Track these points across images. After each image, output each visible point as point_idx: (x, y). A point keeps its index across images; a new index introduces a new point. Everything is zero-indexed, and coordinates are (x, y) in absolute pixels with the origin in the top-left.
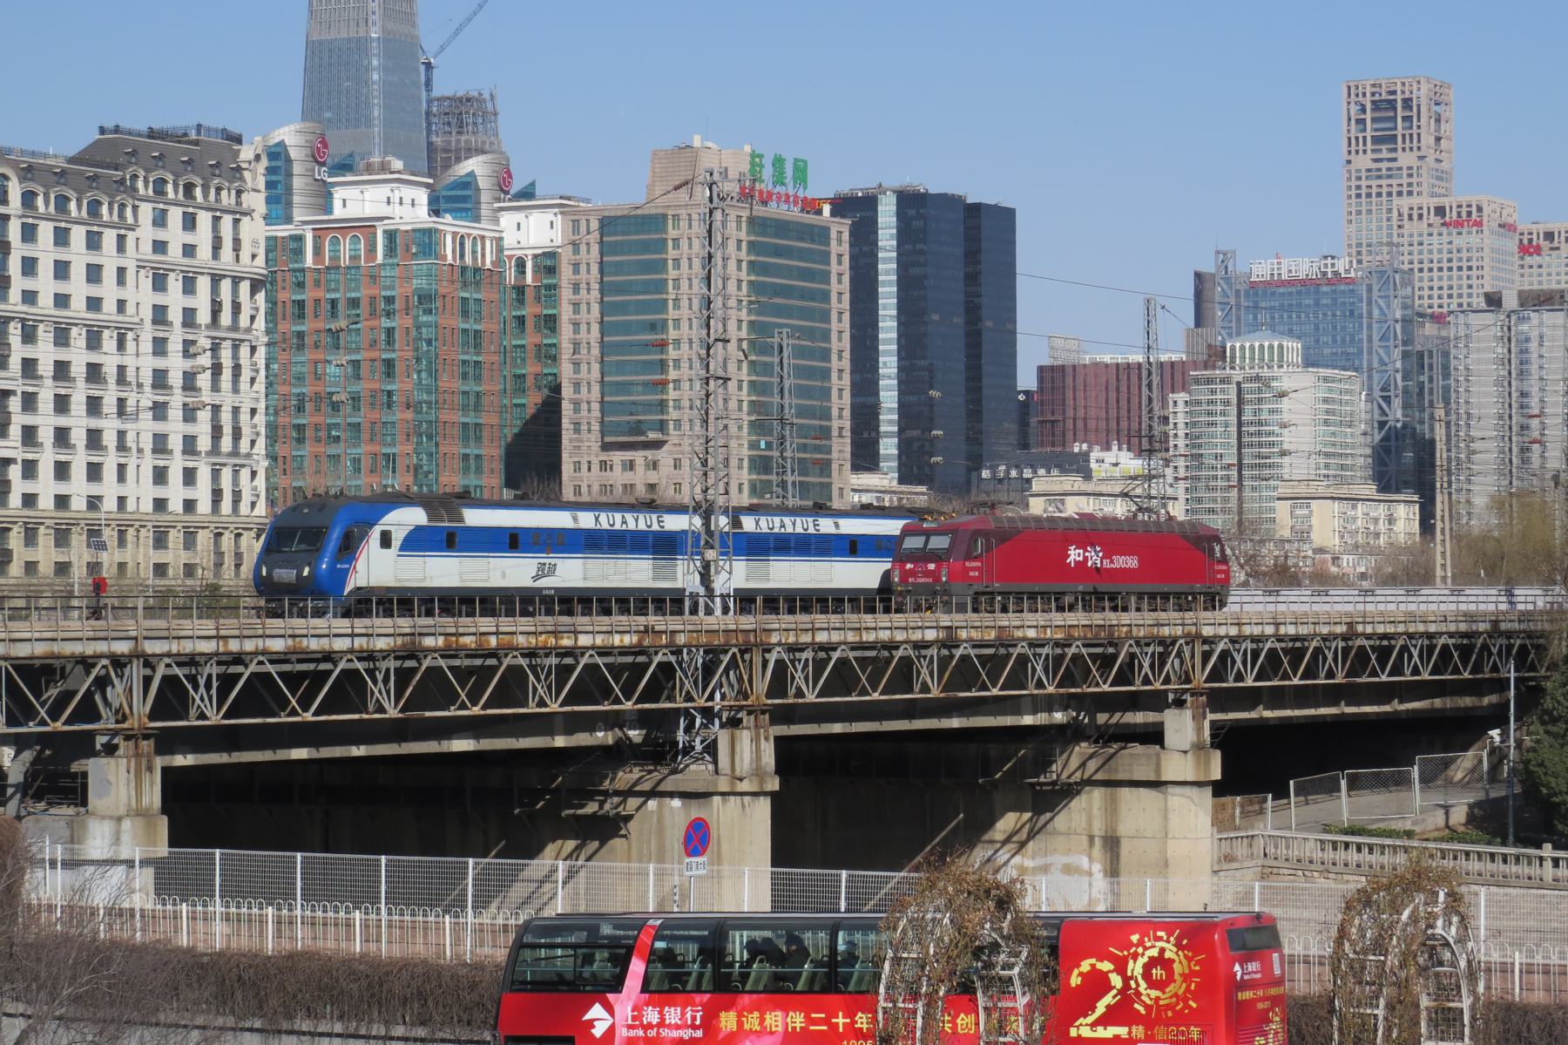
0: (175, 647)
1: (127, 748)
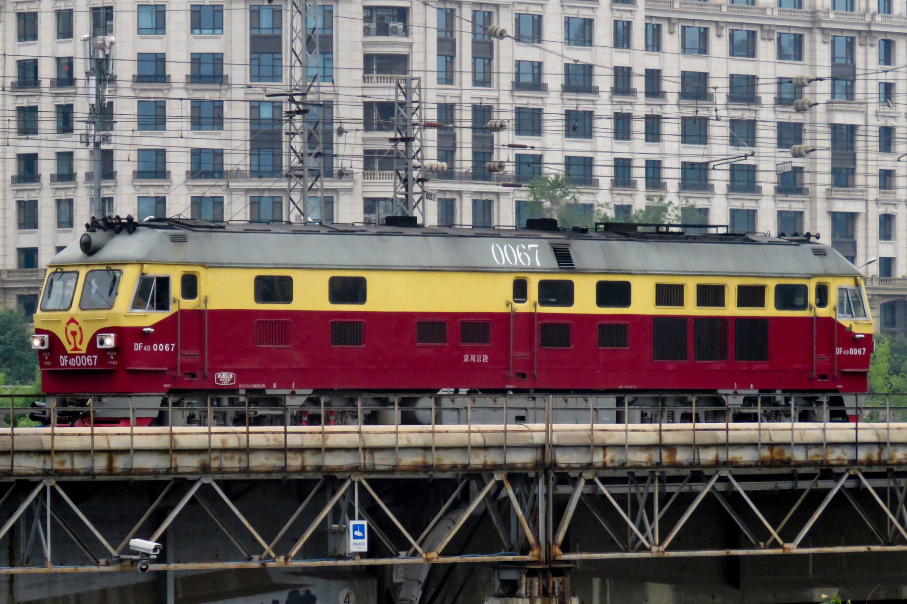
0: (598, 458)
1: (530, 587)
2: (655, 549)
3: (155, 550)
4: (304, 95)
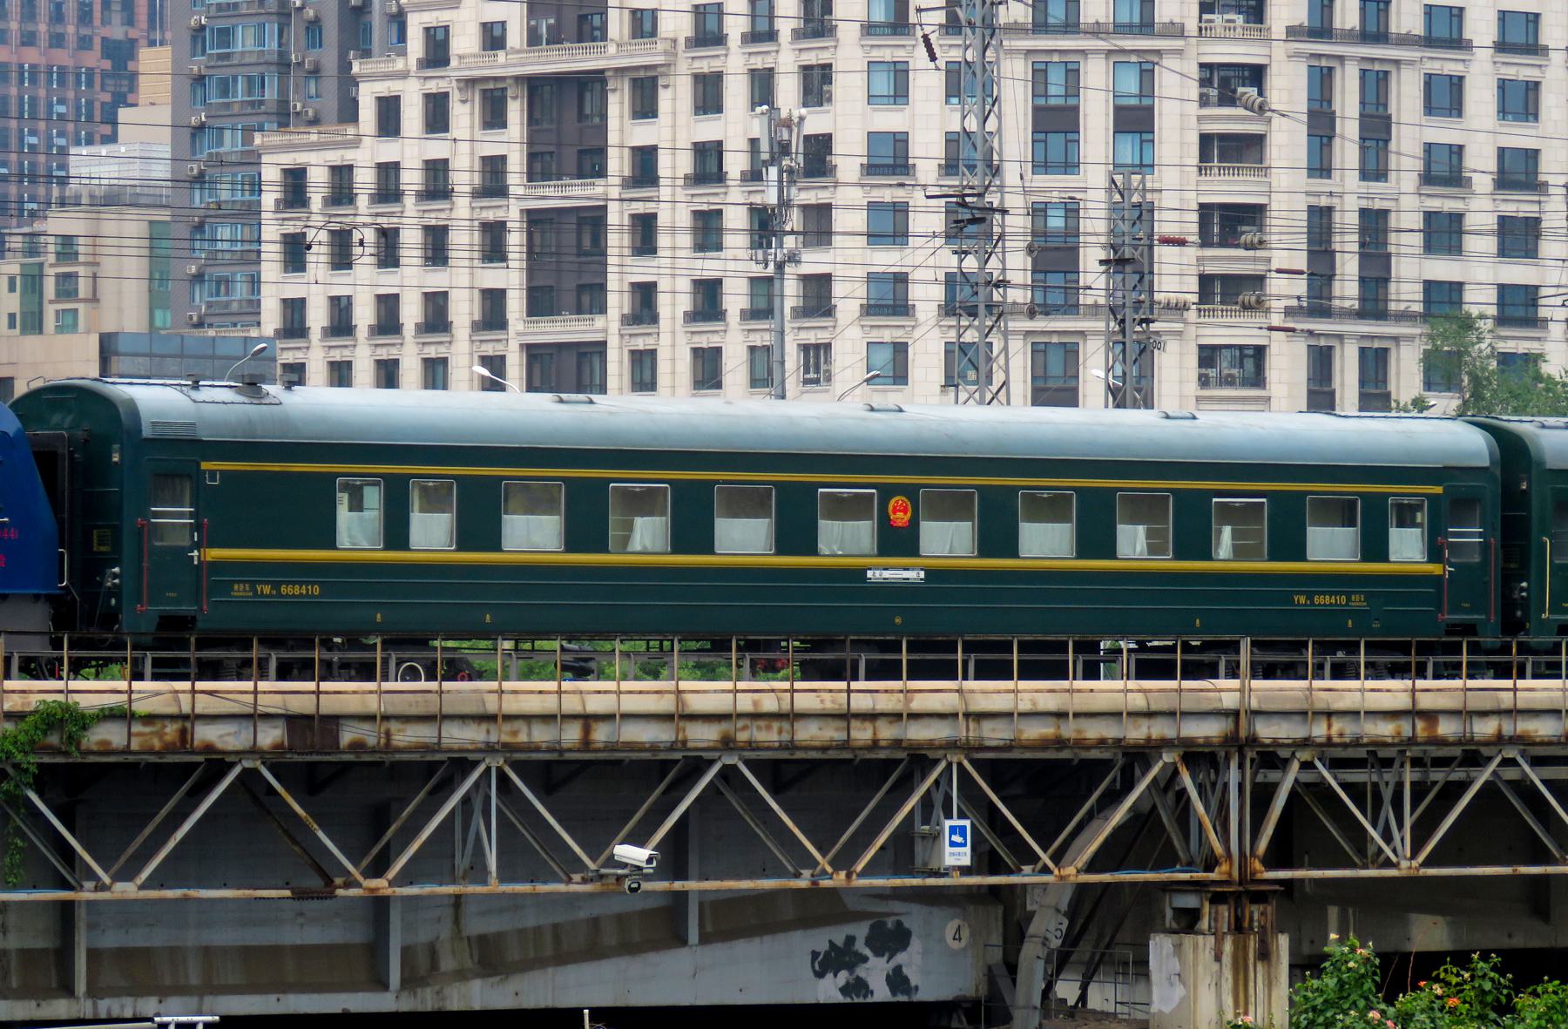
0: (1319, 730)
1: (1215, 918)
2: (1404, 864)
3: (650, 861)
4: (980, 195)
